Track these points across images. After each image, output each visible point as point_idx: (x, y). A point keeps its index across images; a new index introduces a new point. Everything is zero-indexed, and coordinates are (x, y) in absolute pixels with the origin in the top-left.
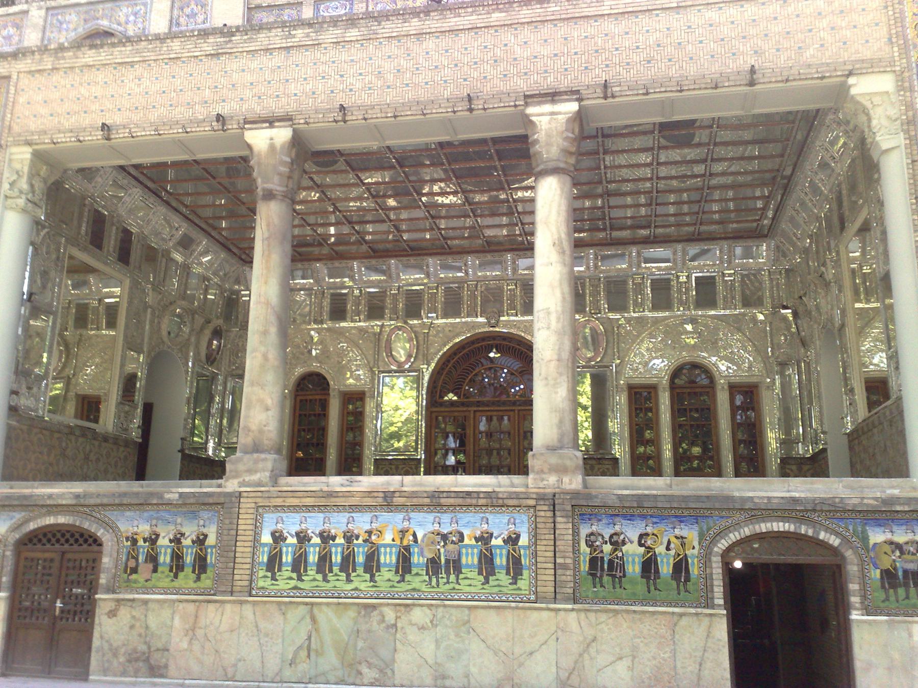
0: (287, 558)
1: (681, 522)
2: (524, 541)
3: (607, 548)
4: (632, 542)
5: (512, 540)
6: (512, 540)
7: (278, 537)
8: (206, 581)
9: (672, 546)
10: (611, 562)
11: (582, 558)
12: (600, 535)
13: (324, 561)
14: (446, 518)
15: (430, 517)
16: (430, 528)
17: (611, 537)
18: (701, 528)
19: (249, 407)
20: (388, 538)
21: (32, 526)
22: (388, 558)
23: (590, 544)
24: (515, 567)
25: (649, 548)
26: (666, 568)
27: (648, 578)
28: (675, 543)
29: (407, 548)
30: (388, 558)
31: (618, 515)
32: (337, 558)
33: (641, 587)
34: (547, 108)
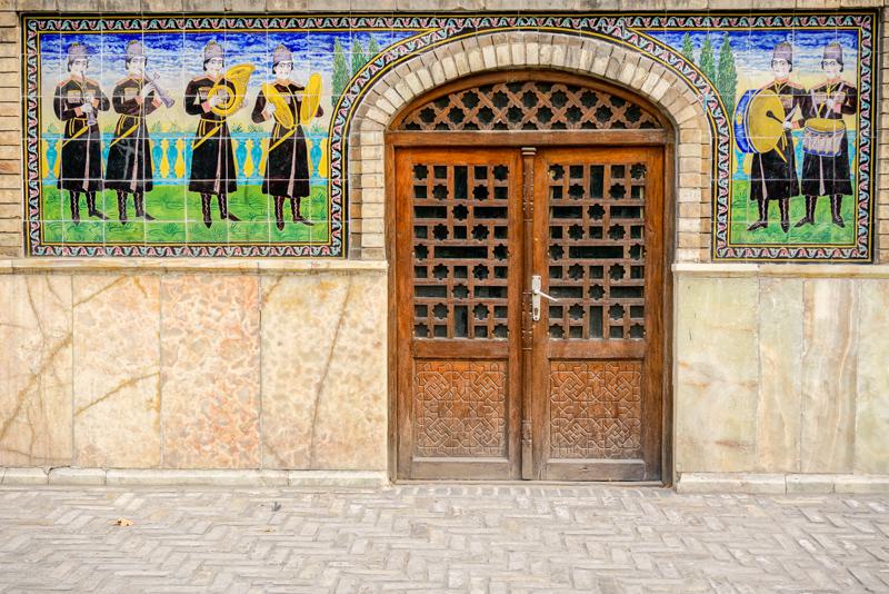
1: (292, 49)
3: (109, 121)
4: (169, 103)
9: (268, 109)
10: (115, 153)
11: (45, 147)
12: (90, 86)
17: (120, 89)
18: (340, 64)
23: (66, 111)
25: (211, 115)
26: (251, 170)
27: (206, 191)
28: (277, 104)
31: (137, 37)
33: (188, 215)
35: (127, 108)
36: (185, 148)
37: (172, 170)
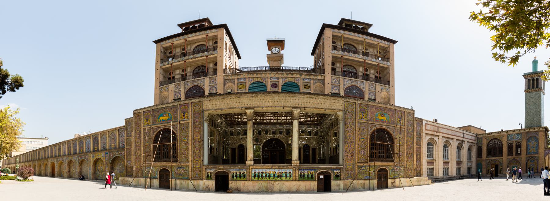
0: (257, 176)
2: (291, 173)
3: (303, 174)
5: (290, 173)
6: (290, 173)
7: (255, 173)
8: (245, 179)
13: (262, 176)
14: (280, 170)
15: (278, 170)
16: (278, 171)
19: (249, 154)
20: (272, 173)
21: (217, 171)
22: (272, 175)
23: (300, 173)
24: (290, 176)
29: (275, 174)
30: (272, 175)
32: (264, 175)
33: (307, 179)
34: (296, 110)
35: (304, 173)
36: (307, 175)
37: (306, 176)
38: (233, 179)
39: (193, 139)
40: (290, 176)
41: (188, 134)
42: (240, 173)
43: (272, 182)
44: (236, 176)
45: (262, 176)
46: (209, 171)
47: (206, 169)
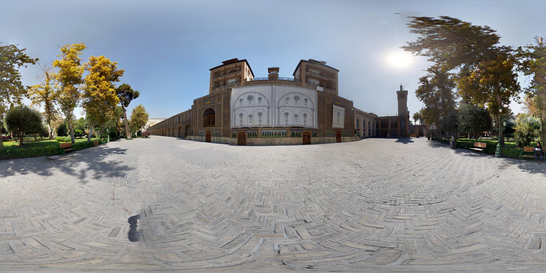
0: (264, 134)
5: (285, 132)
6: (285, 132)
7: (263, 132)
8: (257, 136)
13: (268, 134)
22: (274, 134)
30: (274, 134)
32: (269, 134)
38: (249, 137)
39: (224, 113)
40: (286, 134)
41: (221, 110)
42: (253, 133)
43: (274, 138)
44: (251, 135)
45: (268, 134)
46: (234, 132)
47: (232, 131)
